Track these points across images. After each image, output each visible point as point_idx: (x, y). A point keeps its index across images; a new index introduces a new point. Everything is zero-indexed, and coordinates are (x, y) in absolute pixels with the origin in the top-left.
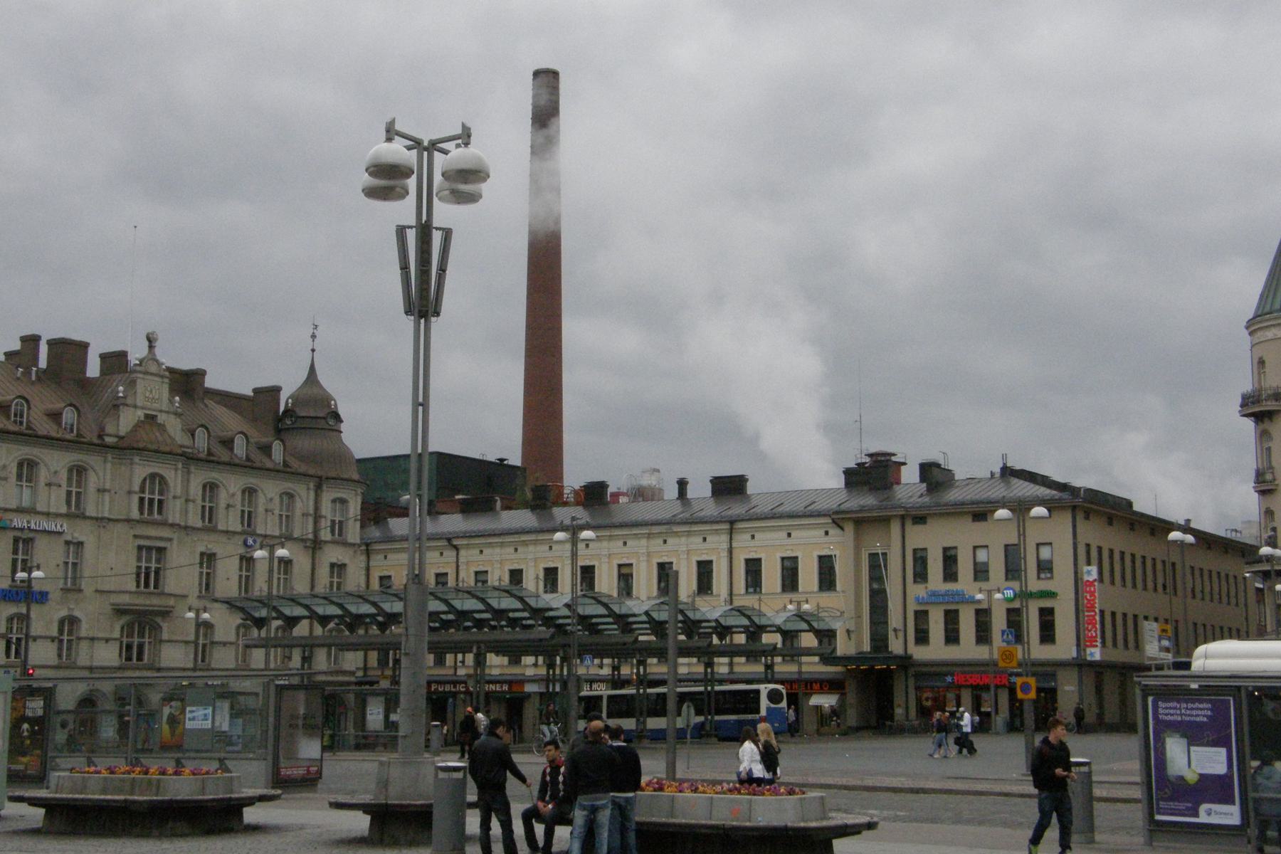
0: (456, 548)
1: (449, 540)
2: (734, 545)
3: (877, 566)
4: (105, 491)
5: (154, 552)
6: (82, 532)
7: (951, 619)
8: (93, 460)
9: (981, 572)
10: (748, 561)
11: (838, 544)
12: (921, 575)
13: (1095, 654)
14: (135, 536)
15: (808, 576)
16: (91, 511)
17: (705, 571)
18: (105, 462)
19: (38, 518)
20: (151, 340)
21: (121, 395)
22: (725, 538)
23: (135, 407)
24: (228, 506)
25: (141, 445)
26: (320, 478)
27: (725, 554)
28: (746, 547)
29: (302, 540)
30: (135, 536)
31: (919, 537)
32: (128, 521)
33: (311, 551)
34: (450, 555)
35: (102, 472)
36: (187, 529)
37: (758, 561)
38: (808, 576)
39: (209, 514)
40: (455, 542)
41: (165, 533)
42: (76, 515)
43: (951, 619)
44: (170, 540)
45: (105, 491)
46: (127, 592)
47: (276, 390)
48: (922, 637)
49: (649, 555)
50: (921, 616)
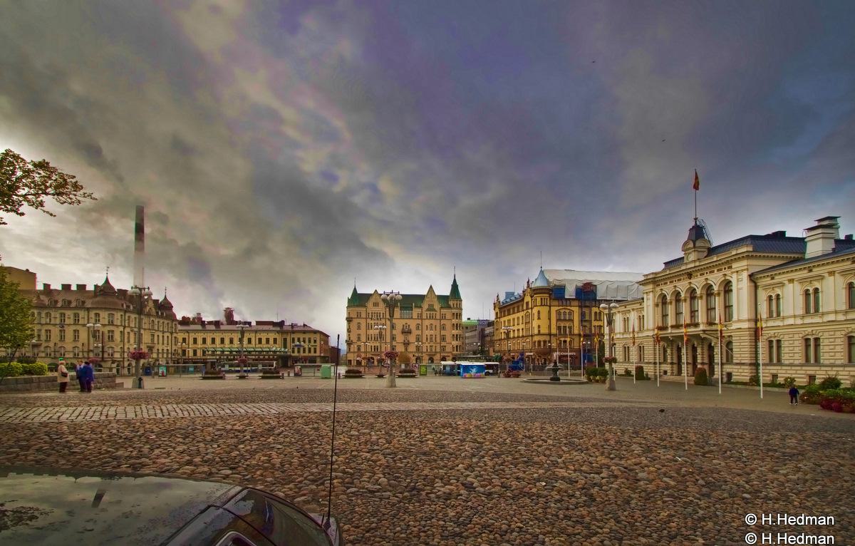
3: (285, 340)
7: (299, 349)
9: (304, 341)
11: (277, 336)
12: (293, 342)
13: (322, 355)
15: (271, 341)
28: (259, 336)
31: (293, 336)
32: (149, 329)
36: (156, 330)
37: (251, 339)
38: (271, 341)
43: (299, 349)
47: (158, 300)
48: (293, 352)
50: (293, 349)
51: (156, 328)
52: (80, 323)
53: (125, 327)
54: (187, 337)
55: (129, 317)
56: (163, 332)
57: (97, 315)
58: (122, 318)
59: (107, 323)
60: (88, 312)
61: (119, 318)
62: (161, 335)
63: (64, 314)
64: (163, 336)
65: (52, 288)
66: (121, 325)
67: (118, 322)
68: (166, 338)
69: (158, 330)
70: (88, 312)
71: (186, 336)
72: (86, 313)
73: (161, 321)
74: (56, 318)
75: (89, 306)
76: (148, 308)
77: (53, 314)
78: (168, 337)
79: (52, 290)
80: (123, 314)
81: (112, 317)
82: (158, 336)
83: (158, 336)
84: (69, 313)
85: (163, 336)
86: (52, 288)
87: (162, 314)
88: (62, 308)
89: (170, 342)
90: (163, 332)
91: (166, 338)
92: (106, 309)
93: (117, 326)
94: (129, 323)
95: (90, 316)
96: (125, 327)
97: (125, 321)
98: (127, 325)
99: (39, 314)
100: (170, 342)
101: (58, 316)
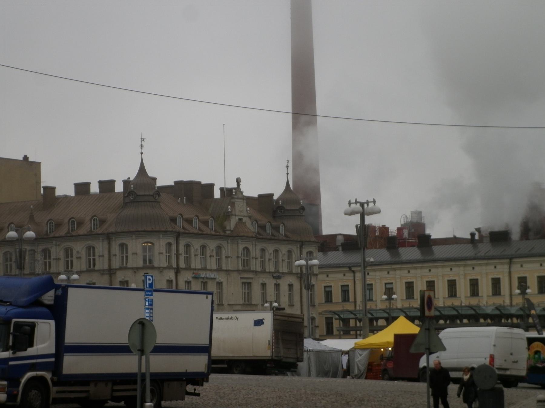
0: (354, 272)
1: (350, 268)
2: (512, 270)
4: (229, 257)
5: (247, 284)
6: (221, 277)
8: (224, 243)
10: (519, 278)
14: (241, 278)
16: (224, 268)
17: (496, 283)
18: (228, 243)
19: (208, 273)
20: (238, 181)
21: (230, 210)
22: (506, 267)
23: (236, 215)
24: (269, 260)
25: (242, 234)
26: (302, 242)
27: (507, 275)
28: (518, 271)
29: (297, 274)
30: (241, 278)
32: (238, 271)
33: (299, 278)
34: (350, 276)
35: (228, 249)
36: (256, 272)
39: (246, 262)
40: (353, 269)
41: (250, 275)
42: (219, 270)
44: (252, 278)
45: (229, 257)
46: (239, 305)
49: (465, 275)
51: (255, 265)
52: (97, 268)
53: (178, 271)
54: (351, 284)
55: (188, 246)
56: (277, 276)
57: (123, 247)
58: (169, 250)
59: (140, 264)
60: (109, 243)
61: (163, 250)
62: (271, 283)
63: (72, 250)
64: (277, 286)
65: (58, 193)
66: (170, 267)
67: (160, 261)
68: (284, 288)
69: (263, 272)
70: (109, 243)
71: (348, 279)
72: (106, 243)
73: (270, 248)
74: (58, 259)
75: (112, 230)
76: (234, 221)
77: (53, 250)
78: (291, 286)
79: (59, 198)
80: (172, 240)
81: (151, 248)
82: (264, 285)
83: (264, 285)
84: (79, 247)
85: (277, 286)
86: (58, 193)
87: (276, 229)
88: (69, 237)
89: (297, 298)
90: (277, 276)
91: (284, 288)
92: (138, 233)
93: (161, 269)
94: (188, 260)
95: (113, 252)
96: (178, 271)
97: (178, 255)
98: (182, 265)
99: (33, 252)
100: (297, 298)
101: (62, 254)
